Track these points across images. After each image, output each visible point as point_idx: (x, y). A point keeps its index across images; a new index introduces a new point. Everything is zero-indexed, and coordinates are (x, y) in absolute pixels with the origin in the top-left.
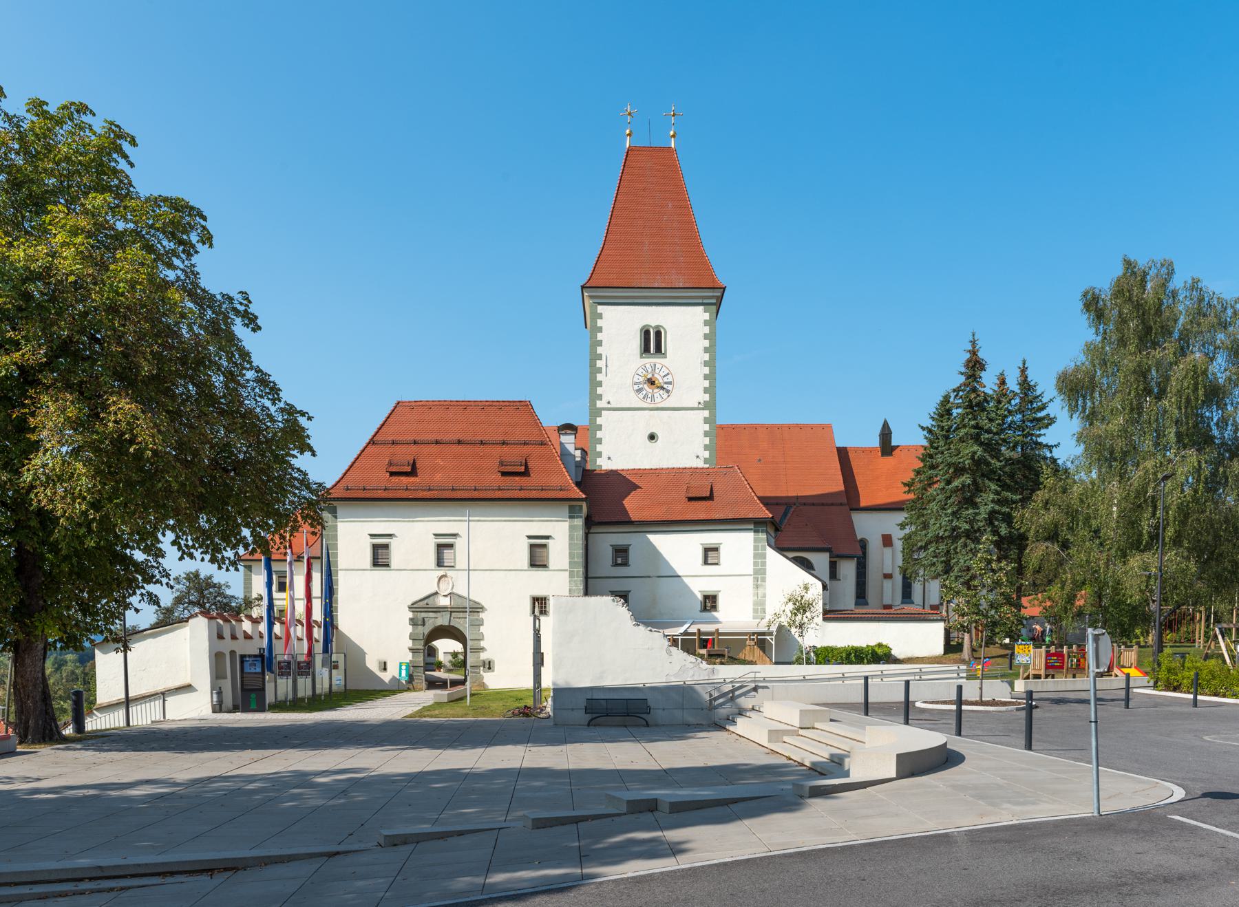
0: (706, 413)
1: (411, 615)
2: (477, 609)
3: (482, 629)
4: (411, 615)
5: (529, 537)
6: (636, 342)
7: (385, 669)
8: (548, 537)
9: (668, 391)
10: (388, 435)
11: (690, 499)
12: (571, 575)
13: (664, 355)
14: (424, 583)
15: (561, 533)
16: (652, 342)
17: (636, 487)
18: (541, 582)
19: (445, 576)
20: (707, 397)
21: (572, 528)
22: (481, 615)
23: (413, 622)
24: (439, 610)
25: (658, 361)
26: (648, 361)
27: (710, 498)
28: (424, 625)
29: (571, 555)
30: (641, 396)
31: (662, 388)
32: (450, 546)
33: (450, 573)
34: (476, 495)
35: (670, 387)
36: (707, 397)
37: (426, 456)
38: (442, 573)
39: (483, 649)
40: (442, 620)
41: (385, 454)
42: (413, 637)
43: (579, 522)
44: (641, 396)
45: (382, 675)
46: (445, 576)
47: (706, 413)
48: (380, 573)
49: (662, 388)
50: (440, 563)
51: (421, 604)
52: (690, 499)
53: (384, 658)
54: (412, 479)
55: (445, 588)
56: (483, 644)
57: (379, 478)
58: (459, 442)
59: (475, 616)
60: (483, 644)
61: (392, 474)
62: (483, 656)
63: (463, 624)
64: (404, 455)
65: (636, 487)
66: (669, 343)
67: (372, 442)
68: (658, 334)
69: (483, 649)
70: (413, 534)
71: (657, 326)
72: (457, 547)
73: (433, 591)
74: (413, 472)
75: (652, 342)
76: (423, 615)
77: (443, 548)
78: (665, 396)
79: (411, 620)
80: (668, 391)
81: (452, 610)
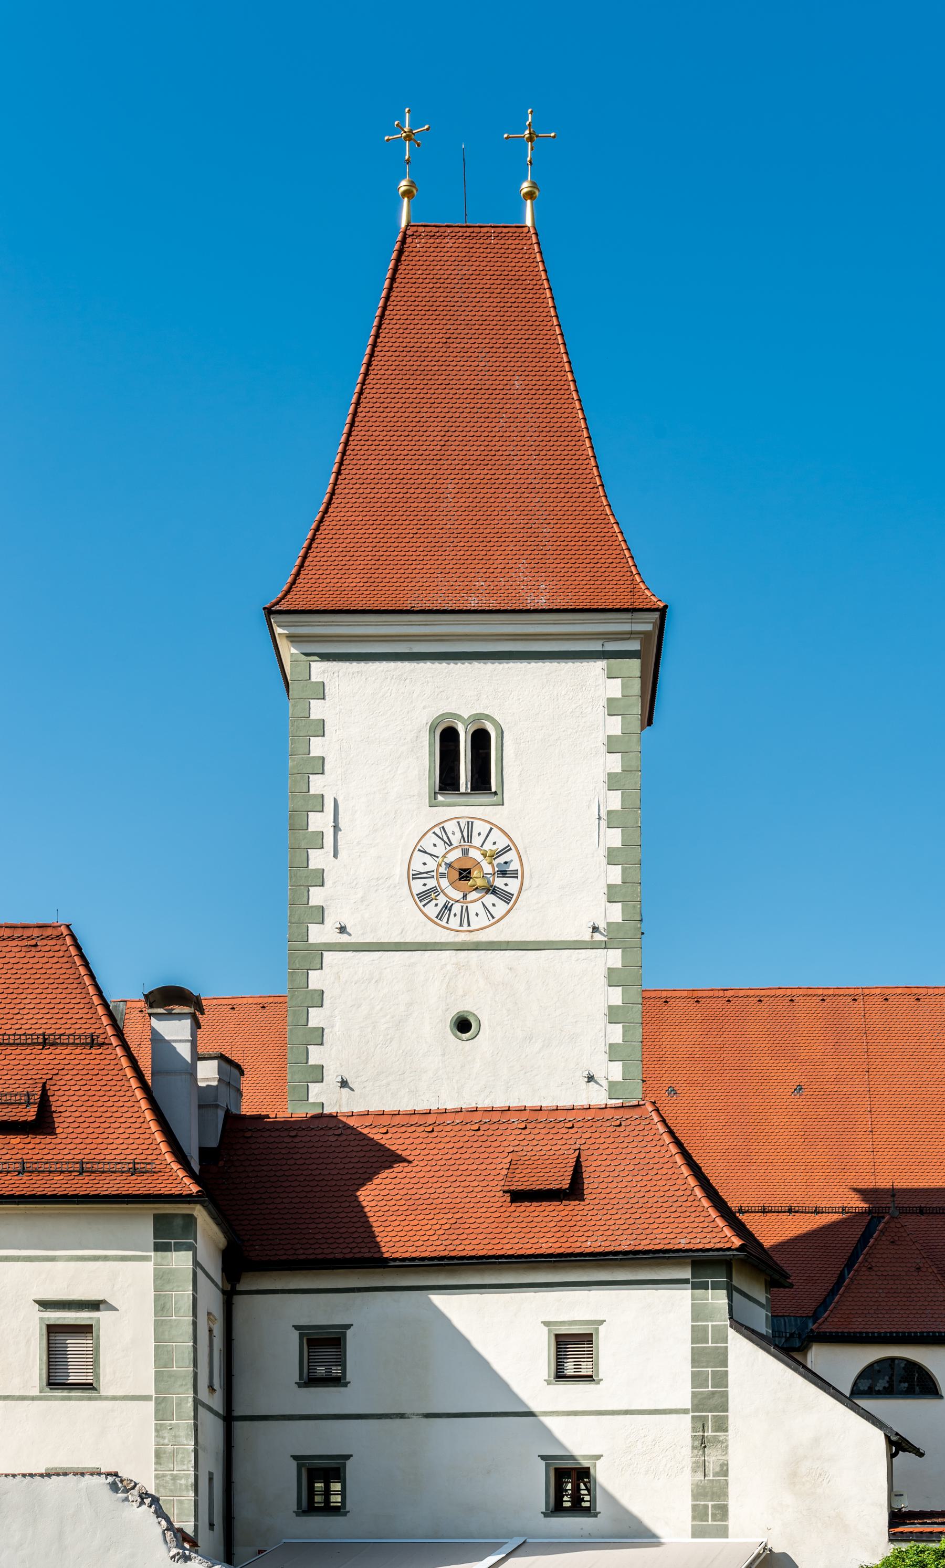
6: (423, 761)
9: (506, 897)
16: (465, 761)
20: (616, 913)
30: (432, 910)
35: (512, 886)
36: (616, 913)
44: (432, 910)
47: (615, 958)
66: (512, 763)
75: (465, 761)
78: (501, 907)
80: (506, 897)
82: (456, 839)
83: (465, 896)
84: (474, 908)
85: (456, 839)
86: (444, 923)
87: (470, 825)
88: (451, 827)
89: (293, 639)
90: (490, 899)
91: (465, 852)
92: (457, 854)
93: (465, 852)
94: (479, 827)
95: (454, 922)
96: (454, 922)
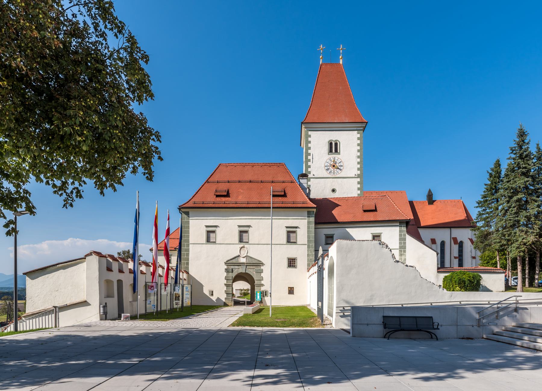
0: (359, 180)
1: (226, 267)
2: (259, 264)
3: (262, 275)
4: (226, 267)
5: (287, 227)
6: (326, 148)
7: (212, 295)
8: (296, 227)
9: (341, 170)
10: (215, 178)
11: (365, 211)
12: (309, 247)
13: (339, 154)
14: (233, 251)
15: (303, 225)
16: (333, 148)
17: (338, 205)
18: (292, 251)
19: (244, 247)
20: (359, 172)
21: (309, 223)
22: (262, 268)
23: (227, 271)
24: (240, 264)
25: (336, 156)
26: (332, 156)
27: (375, 210)
28: (232, 272)
29: (309, 237)
30: (328, 172)
31: (338, 168)
32: (246, 232)
33: (246, 246)
34: (260, 205)
35: (342, 168)
36: (359, 172)
37: (233, 188)
39: (263, 285)
40: (242, 270)
41: (214, 187)
42: (227, 278)
43: (312, 219)
44: (328, 172)
45: (211, 297)
46: (244, 247)
47: (359, 180)
48: (210, 246)
49: (338, 168)
50: (241, 240)
51: (231, 262)
52: (365, 211)
53: (211, 289)
54: (227, 199)
55: (244, 253)
56: (262, 282)
57: (211, 198)
58: (250, 182)
59: (258, 268)
60: (262, 282)
61: (217, 196)
62: (263, 289)
63: (251, 271)
64: (223, 187)
65: (338, 205)
66: (342, 148)
67: (207, 182)
68: (336, 144)
69: (263, 285)
70: (228, 226)
71: (336, 140)
72: (250, 232)
73: (237, 255)
74: (228, 195)
75: (333, 148)
76: (232, 267)
77: (243, 234)
79: (226, 269)
80: (341, 170)
81: (247, 265)
88: (332, 158)
89: (305, 128)
90: (338, 170)
94: (336, 158)
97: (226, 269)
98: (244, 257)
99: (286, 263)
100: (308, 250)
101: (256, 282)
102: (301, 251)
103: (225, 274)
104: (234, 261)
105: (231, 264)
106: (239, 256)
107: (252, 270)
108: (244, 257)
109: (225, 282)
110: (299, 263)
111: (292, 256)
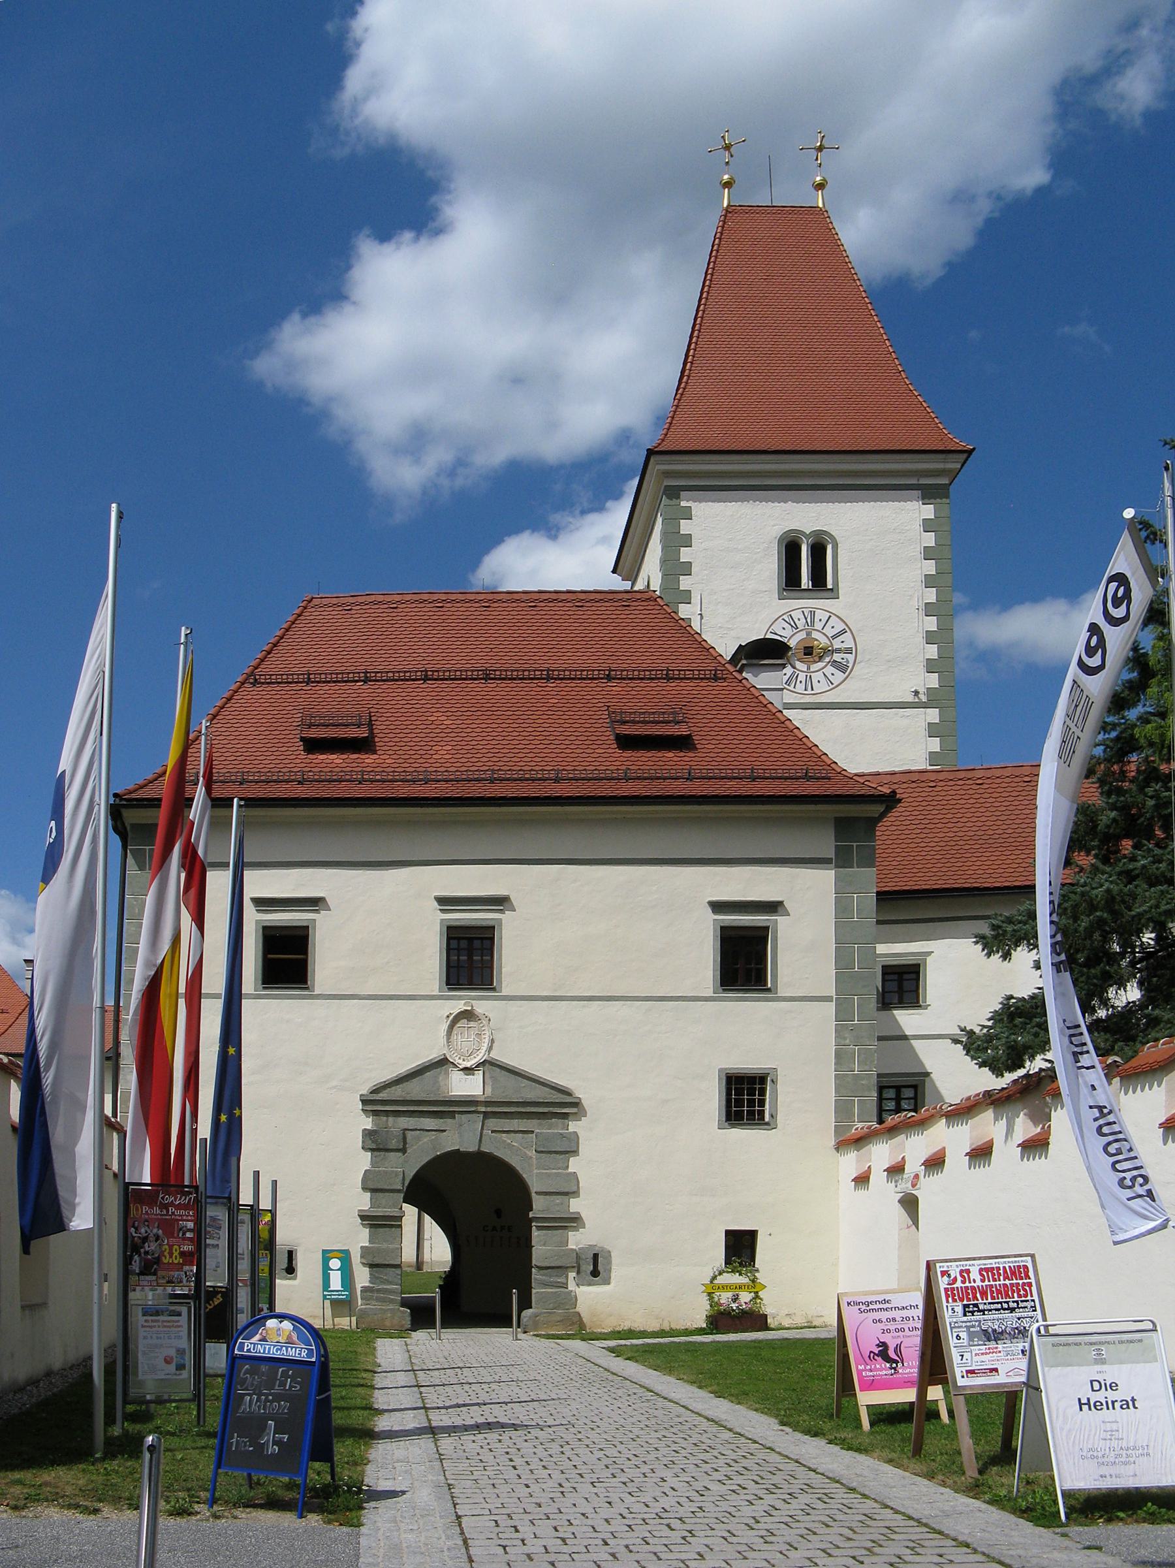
1: (368, 1123)
3: (574, 1165)
4: (368, 1123)
19: (468, 1015)
22: (573, 1126)
23: (375, 1143)
33: (483, 1005)
38: (459, 1006)
39: (575, 1221)
40: (460, 1137)
42: (372, 1185)
51: (397, 1093)
55: (469, 1047)
56: (575, 1205)
60: (575, 1205)
62: (576, 1240)
63: (515, 1148)
69: (575, 1221)
73: (433, 1055)
76: (404, 1122)
79: (367, 1134)
81: (488, 1110)
82: (801, 624)
83: (809, 668)
84: (816, 677)
85: (801, 624)
86: (791, 688)
87: (813, 614)
91: (809, 634)
92: (803, 635)
93: (809, 634)
94: (819, 615)
95: (800, 688)
96: (800, 688)
97: (367, 1134)
98: (468, 1070)
99: (712, 1099)
100: (838, 1031)
101: (539, 1206)
102: (796, 1034)
103: (365, 1160)
104: (415, 1090)
105: (395, 1105)
106: (443, 1062)
107: (515, 1141)
108: (468, 1070)
109: (364, 1201)
110: (784, 1099)
111: (746, 1062)
